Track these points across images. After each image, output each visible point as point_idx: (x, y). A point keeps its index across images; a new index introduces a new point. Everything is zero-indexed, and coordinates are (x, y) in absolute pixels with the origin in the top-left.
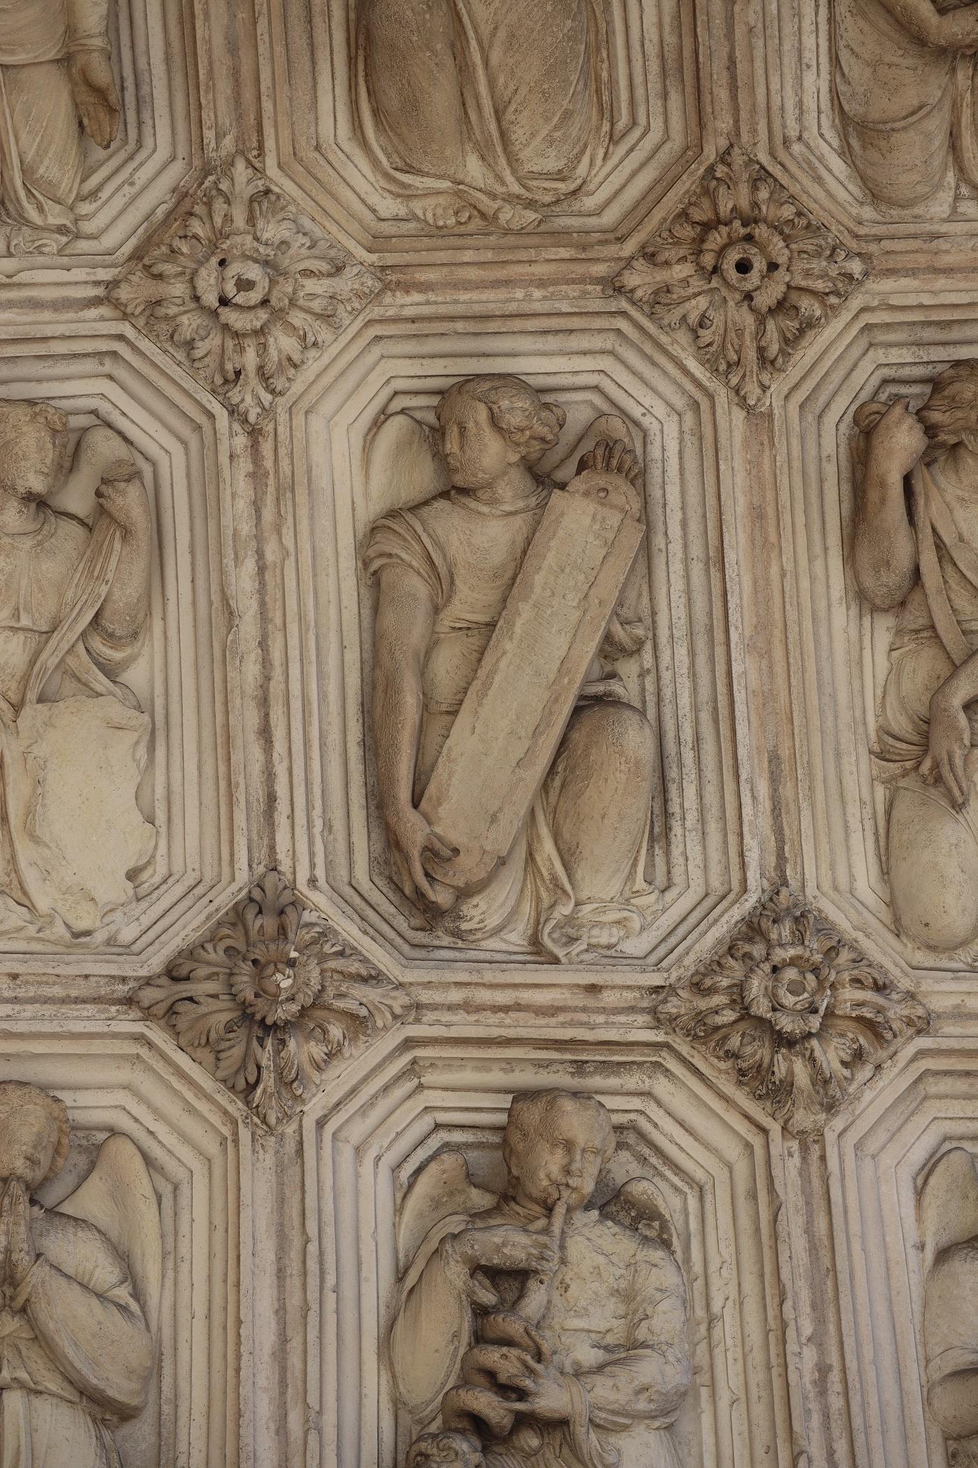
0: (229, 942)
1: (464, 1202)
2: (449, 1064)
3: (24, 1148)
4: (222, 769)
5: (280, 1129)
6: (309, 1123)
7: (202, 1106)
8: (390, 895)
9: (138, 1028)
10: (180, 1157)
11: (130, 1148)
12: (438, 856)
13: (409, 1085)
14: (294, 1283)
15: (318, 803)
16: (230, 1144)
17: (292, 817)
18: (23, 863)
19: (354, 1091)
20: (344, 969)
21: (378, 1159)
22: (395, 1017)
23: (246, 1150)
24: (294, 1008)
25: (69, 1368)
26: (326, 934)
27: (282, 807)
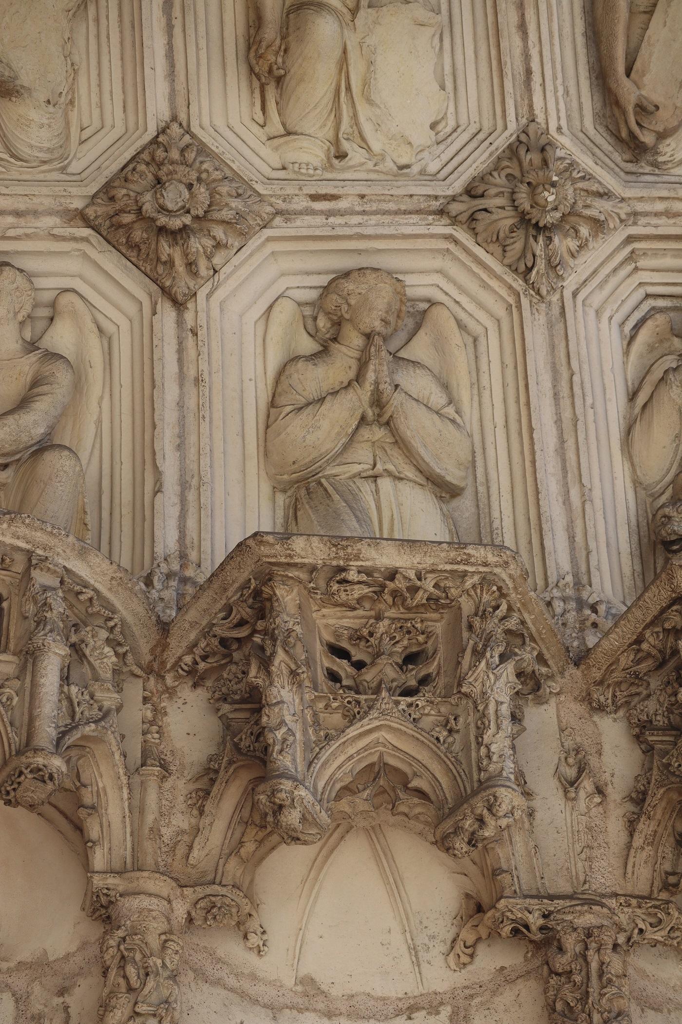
0: (509, 171)
1: (670, 347)
2: (656, 253)
3: (380, 313)
4: (494, 52)
5: (548, 298)
6: (568, 294)
7: (494, 283)
8: (608, 138)
9: (448, 230)
10: (480, 320)
11: (446, 313)
12: (643, 109)
13: (629, 268)
14: (566, 403)
15: (560, 75)
16: (514, 310)
17: (543, 84)
18: (362, 118)
19: (595, 272)
20: (589, 188)
21: (611, 318)
22: (622, 221)
23: (526, 313)
24: (558, 215)
25: (420, 462)
26: (572, 165)
27: (536, 78)
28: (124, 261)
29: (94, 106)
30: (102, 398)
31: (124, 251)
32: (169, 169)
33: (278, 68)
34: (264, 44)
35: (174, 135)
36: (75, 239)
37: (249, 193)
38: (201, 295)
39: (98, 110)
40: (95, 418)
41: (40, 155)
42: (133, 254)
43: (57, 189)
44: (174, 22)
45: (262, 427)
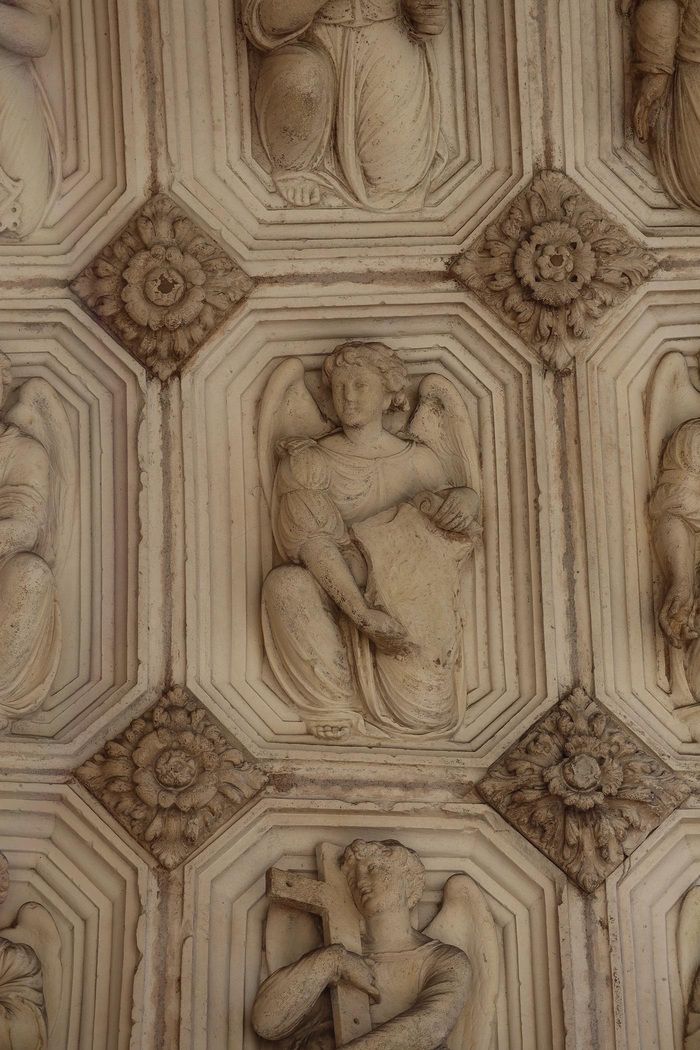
28: (525, 842)
29: (481, 665)
30: (497, 996)
31: (525, 832)
32: (578, 741)
33: (691, 631)
34: (678, 603)
35: (578, 702)
36: (468, 816)
37: (662, 769)
38: (611, 882)
39: (486, 671)
40: (491, 1018)
42: (535, 835)
43: (449, 759)
44: (576, 576)
45: (679, 1034)
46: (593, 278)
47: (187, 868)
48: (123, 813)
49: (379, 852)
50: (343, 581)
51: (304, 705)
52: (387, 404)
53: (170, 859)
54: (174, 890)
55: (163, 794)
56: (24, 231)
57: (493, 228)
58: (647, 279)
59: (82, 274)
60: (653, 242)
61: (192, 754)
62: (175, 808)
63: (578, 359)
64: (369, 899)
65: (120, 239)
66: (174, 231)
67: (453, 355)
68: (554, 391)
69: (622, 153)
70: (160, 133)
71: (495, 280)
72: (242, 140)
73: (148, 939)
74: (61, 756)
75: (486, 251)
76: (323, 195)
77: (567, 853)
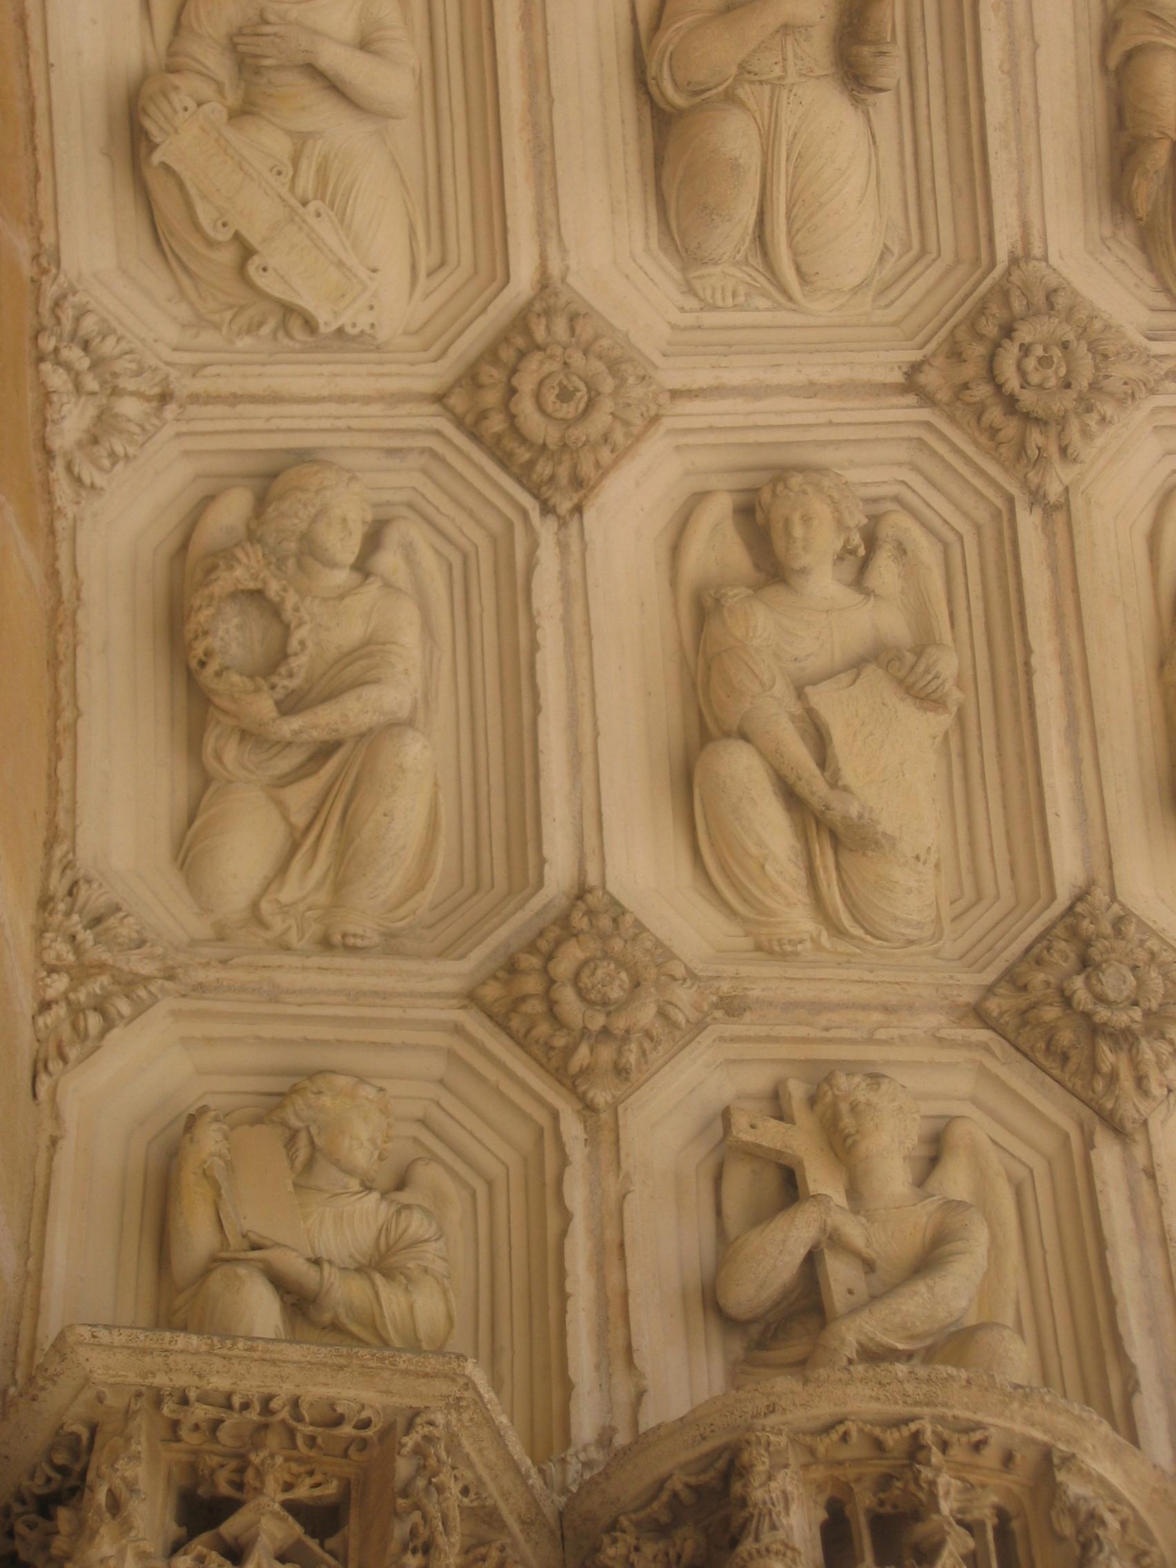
29: (964, 871)
36: (967, 1044)
41: (907, 931)
42: (1052, 1065)
46: (1093, 386)
47: (620, 1109)
48: (537, 1042)
49: (863, 1085)
50: (799, 753)
51: (751, 915)
52: (839, 545)
53: (601, 1097)
54: (606, 1136)
55: (589, 1013)
56: (382, 335)
57: (963, 327)
58: (1153, 392)
59: (458, 382)
60: (1158, 348)
61: (621, 965)
62: (605, 1031)
63: (1071, 490)
64: (855, 1143)
65: (504, 337)
66: (572, 330)
67: (914, 491)
68: (1043, 529)
69: (1111, 243)
70: (550, 213)
71: (968, 389)
72: (647, 228)
73: (577, 1195)
74: (453, 974)
75: (956, 354)
76: (747, 295)
77: (1100, 1085)
